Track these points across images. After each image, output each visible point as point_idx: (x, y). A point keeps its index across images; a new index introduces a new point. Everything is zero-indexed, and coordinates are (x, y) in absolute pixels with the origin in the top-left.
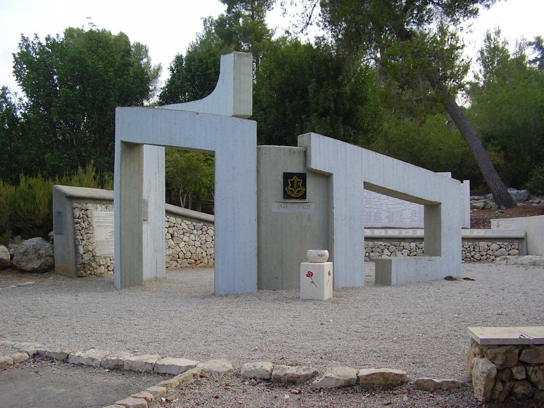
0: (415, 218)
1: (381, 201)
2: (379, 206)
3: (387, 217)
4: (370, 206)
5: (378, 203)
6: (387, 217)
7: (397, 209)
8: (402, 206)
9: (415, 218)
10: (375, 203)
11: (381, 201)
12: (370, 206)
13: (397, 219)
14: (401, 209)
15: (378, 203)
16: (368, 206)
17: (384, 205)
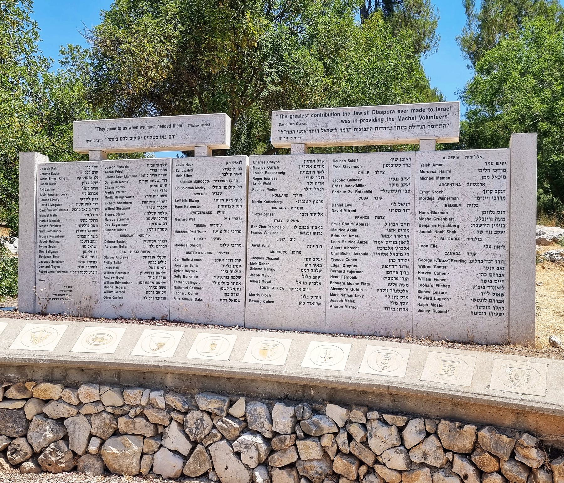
0: (315, 290)
1: (200, 219)
2: (190, 239)
3: (218, 280)
4: (164, 235)
5: (190, 225)
6: (218, 280)
7: (253, 252)
8: (271, 239)
9: (315, 290)
10: (177, 226)
11: (200, 219)
12: (164, 235)
13: (254, 288)
14: (265, 252)
15: (190, 225)
16: (156, 235)
17: (210, 233)
